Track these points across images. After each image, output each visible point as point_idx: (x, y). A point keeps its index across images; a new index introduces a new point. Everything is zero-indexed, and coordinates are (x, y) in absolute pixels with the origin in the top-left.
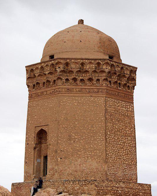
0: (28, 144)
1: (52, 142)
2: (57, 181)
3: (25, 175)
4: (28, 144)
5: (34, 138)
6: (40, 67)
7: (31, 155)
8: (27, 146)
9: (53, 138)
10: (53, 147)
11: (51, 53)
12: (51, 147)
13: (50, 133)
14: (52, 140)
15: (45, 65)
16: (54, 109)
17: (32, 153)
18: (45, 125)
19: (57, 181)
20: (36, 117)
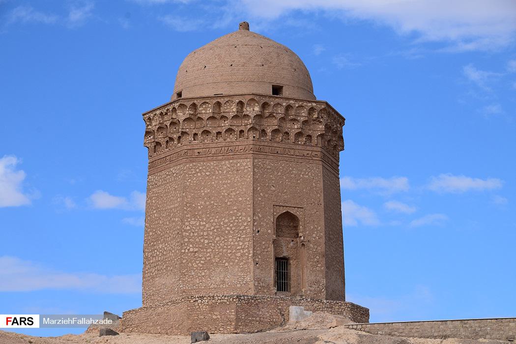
0: (258, 231)
1: (315, 238)
2: (338, 303)
3: (256, 284)
4: (258, 231)
5: (272, 224)
6: (284, 104)
7: (267, 252)
8: (257, 234)
9: (315, 232)
10: (316, 247)
11: (278, 82)
12: (311, 245)
13: (308, 223)
14: (314, 235)
15: (297, 105)
16: (314, 184)
17: (269, 249)
18: (295, 207)
19: (338, 303)
20: (274, 189)
